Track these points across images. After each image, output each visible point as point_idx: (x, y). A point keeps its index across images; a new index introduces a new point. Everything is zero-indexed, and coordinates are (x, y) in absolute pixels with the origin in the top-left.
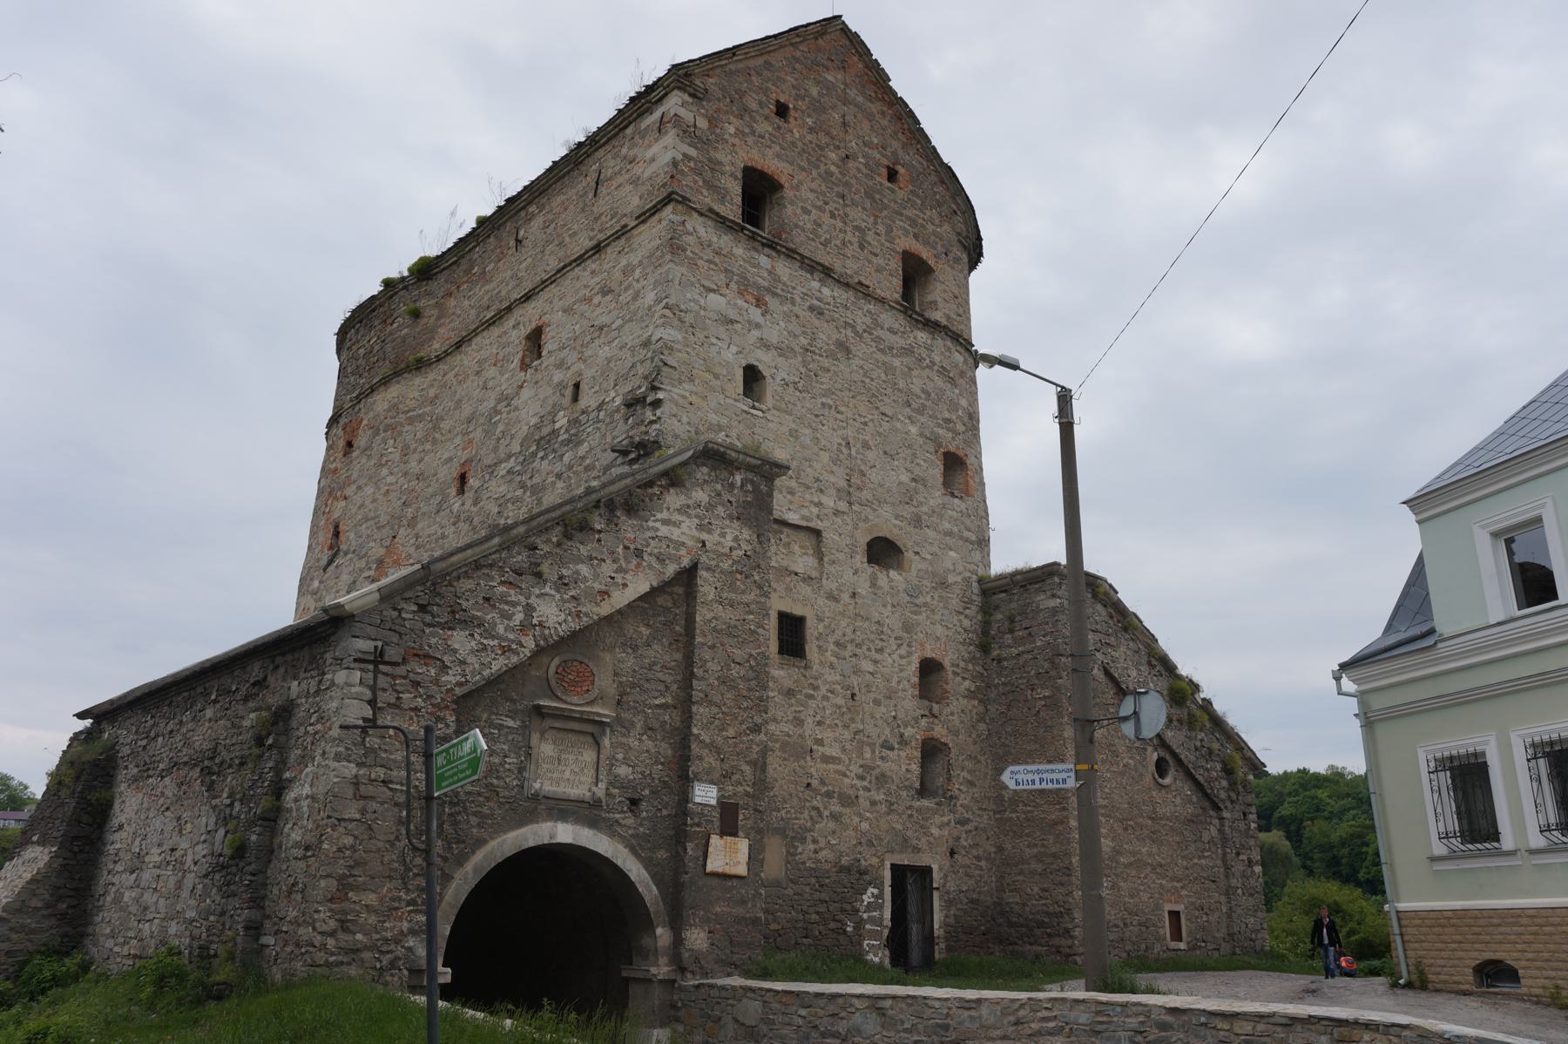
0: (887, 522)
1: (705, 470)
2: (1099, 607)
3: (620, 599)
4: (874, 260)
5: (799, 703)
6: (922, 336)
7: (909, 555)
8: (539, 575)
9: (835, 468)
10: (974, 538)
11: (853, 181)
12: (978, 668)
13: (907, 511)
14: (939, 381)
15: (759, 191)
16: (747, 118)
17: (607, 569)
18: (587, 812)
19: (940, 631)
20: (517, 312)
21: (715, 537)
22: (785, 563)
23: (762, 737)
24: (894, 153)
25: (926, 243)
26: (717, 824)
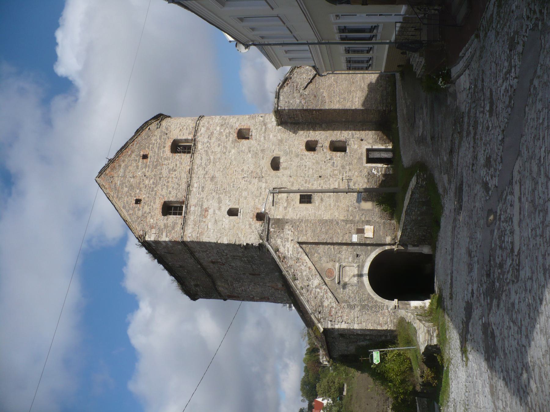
0: (266, 164)
1: (272, 240)
3: (310, 264)
4: (178, 165)
6: (199, 146)
7: (275, 154)
8: (308, 286)
9: (253, 183)
10: (264, 127)
11: (153, 173)
12: (306, 126)
13: (261, 155)
14: (213, 140)
16: (146, 215)
17: (303, 268)
18: (360, 267)
19: (296, 143)
21: (289, 236)
22: (285, 200)
23: (339, 221)
24: (137, 156)
25: (165, 143)
26: (362, 235)
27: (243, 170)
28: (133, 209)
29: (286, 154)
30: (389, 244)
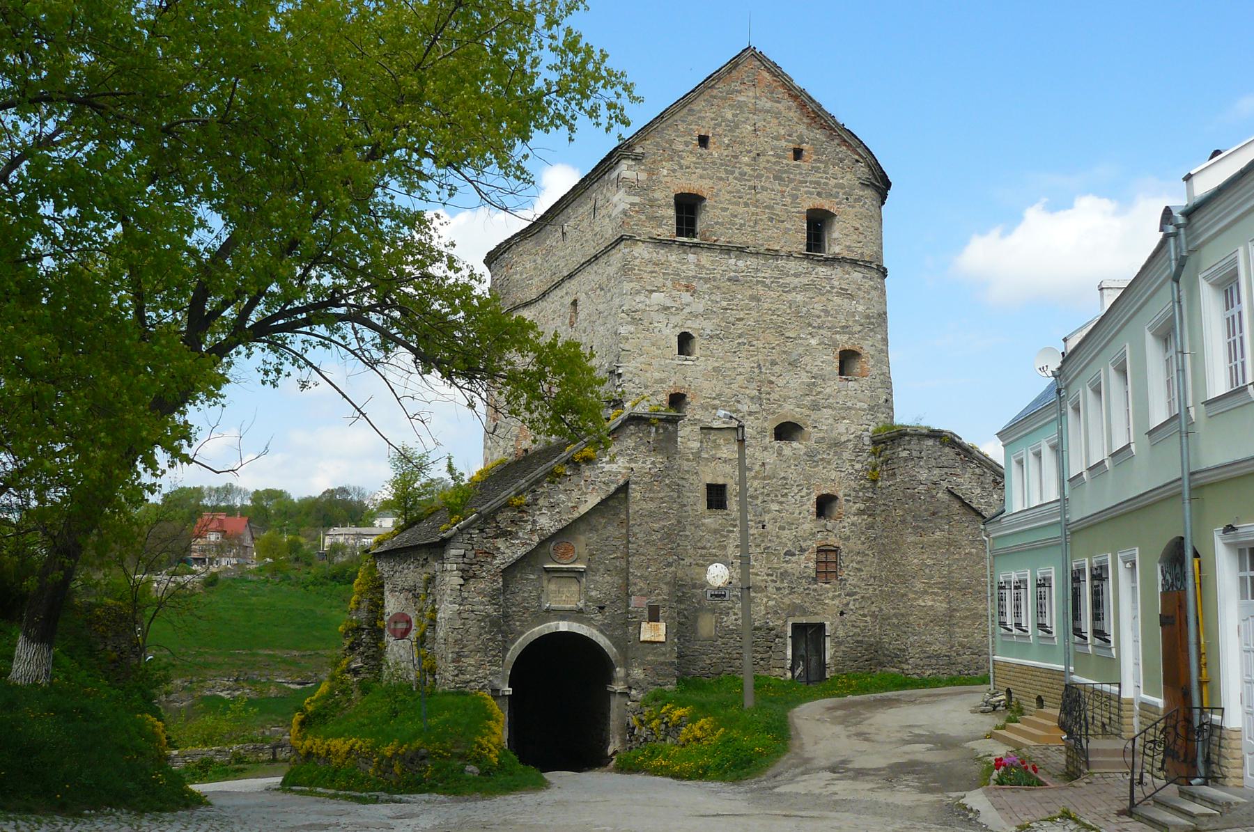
0: (790, 411)
2: (947, 449)
3: (583, 509)
5: (723, 536)
6: (822, 270)
10: (866, 406)
14: (837, 300)
15: (688, 208)
17: (575, 494)
18: (576, 615)
19: (833, 475)
20: (566, 284)
24: (800, 137)
27: (774, 363)
28: (689, 133)
29: (811, 455)
30: (628, 675)
